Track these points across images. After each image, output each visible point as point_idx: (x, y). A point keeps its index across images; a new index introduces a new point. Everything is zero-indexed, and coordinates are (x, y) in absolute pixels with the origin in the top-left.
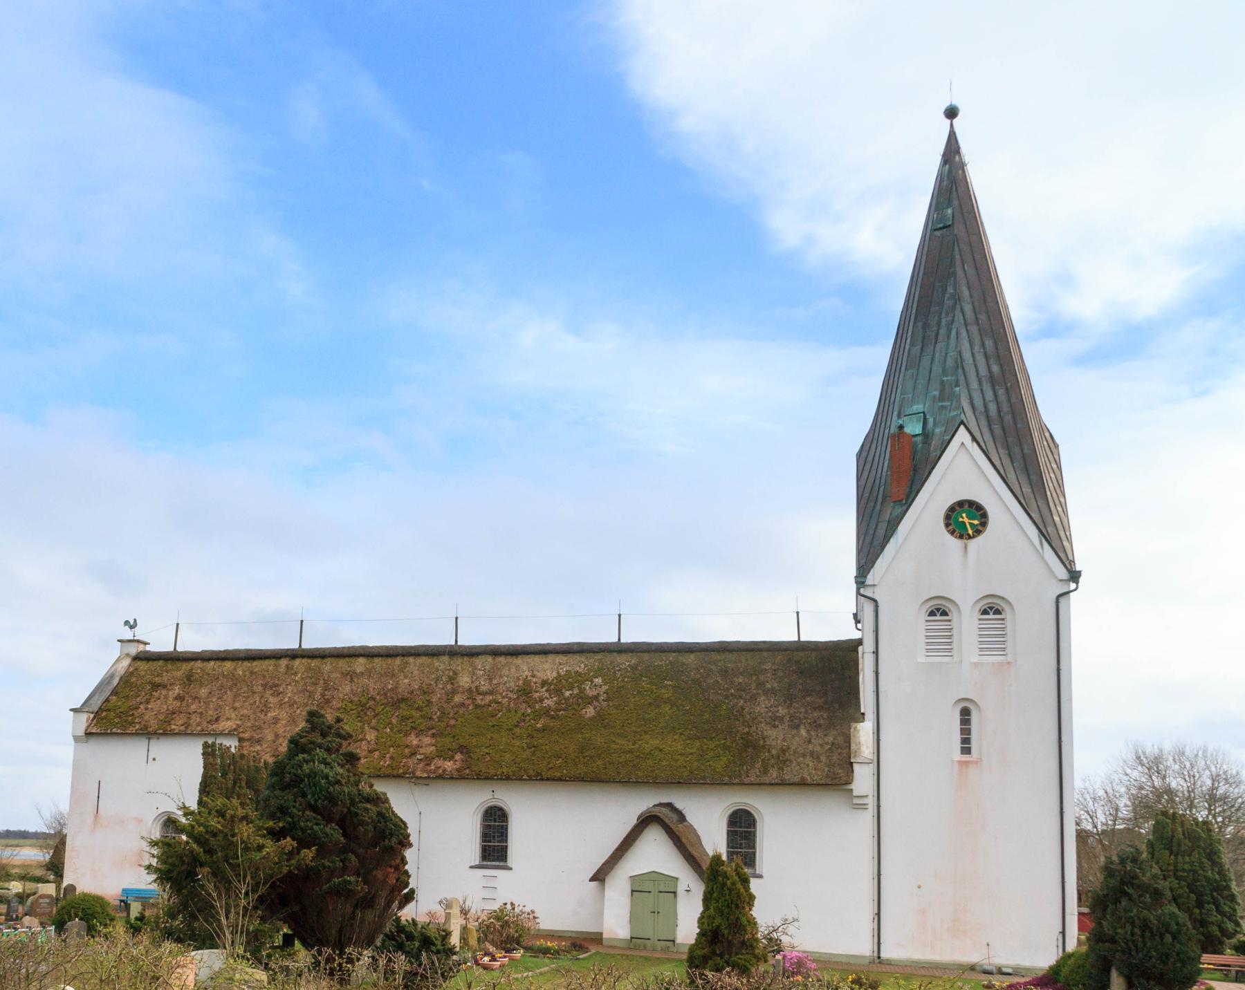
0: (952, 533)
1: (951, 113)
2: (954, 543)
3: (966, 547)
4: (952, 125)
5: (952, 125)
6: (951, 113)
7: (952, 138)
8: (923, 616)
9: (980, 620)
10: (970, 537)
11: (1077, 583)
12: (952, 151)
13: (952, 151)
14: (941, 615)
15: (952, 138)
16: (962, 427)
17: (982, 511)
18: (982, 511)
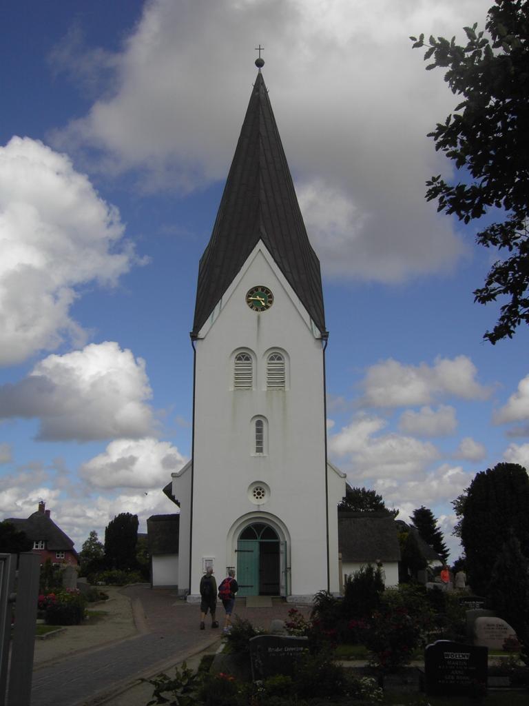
0: (251, 307)
1: (260, 63)
2: (253, 314)
3: (259, 318)
4: (260, 70)
5: (260, 70)
6: (260, 63)
7: (260, 77)
8: (233, 360)
9: (269, 364)
10: (263, 309)
11: (326, 340)
12: (259, 85)
13: (259, 85)
14: (245, 360)
15: (260, 77)
16: (260, 240)
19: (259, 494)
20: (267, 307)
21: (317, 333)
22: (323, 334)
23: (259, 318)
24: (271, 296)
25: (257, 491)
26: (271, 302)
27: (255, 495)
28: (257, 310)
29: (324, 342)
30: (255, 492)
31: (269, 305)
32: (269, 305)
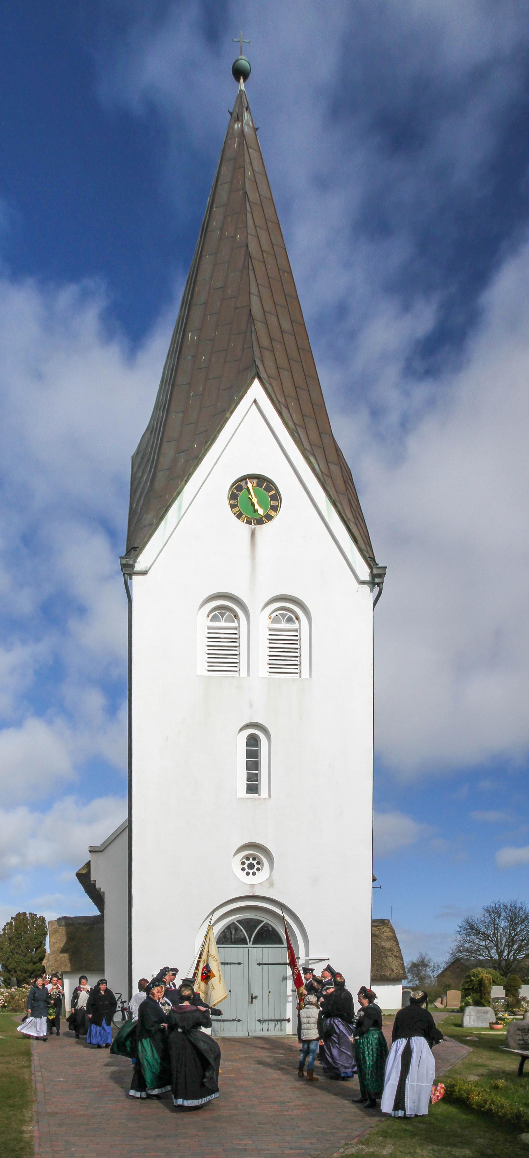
0: (239, 516)
2: (243, 528)
3: (253, 534)
10: (260, 522)
17: (273, 492)
18: (273, 492)
19: (251, 866)
20: (269, 518)
21: (364, 573)
22: (375, 572)
23: (253, 534)
24: (277, 497)
25: (247, 863)
26: (275, 509)
27: (243, 869)
28: (249, 522)
29: (377, 589)
30: (243, 863)
31: (272, 513)
32: (272, 513)
